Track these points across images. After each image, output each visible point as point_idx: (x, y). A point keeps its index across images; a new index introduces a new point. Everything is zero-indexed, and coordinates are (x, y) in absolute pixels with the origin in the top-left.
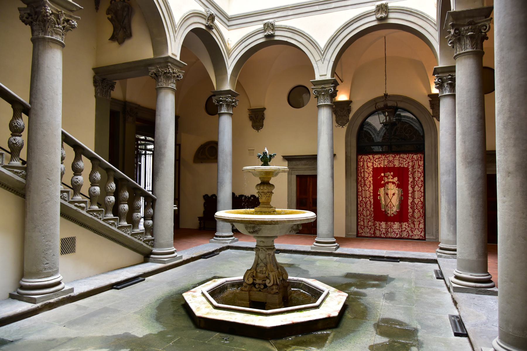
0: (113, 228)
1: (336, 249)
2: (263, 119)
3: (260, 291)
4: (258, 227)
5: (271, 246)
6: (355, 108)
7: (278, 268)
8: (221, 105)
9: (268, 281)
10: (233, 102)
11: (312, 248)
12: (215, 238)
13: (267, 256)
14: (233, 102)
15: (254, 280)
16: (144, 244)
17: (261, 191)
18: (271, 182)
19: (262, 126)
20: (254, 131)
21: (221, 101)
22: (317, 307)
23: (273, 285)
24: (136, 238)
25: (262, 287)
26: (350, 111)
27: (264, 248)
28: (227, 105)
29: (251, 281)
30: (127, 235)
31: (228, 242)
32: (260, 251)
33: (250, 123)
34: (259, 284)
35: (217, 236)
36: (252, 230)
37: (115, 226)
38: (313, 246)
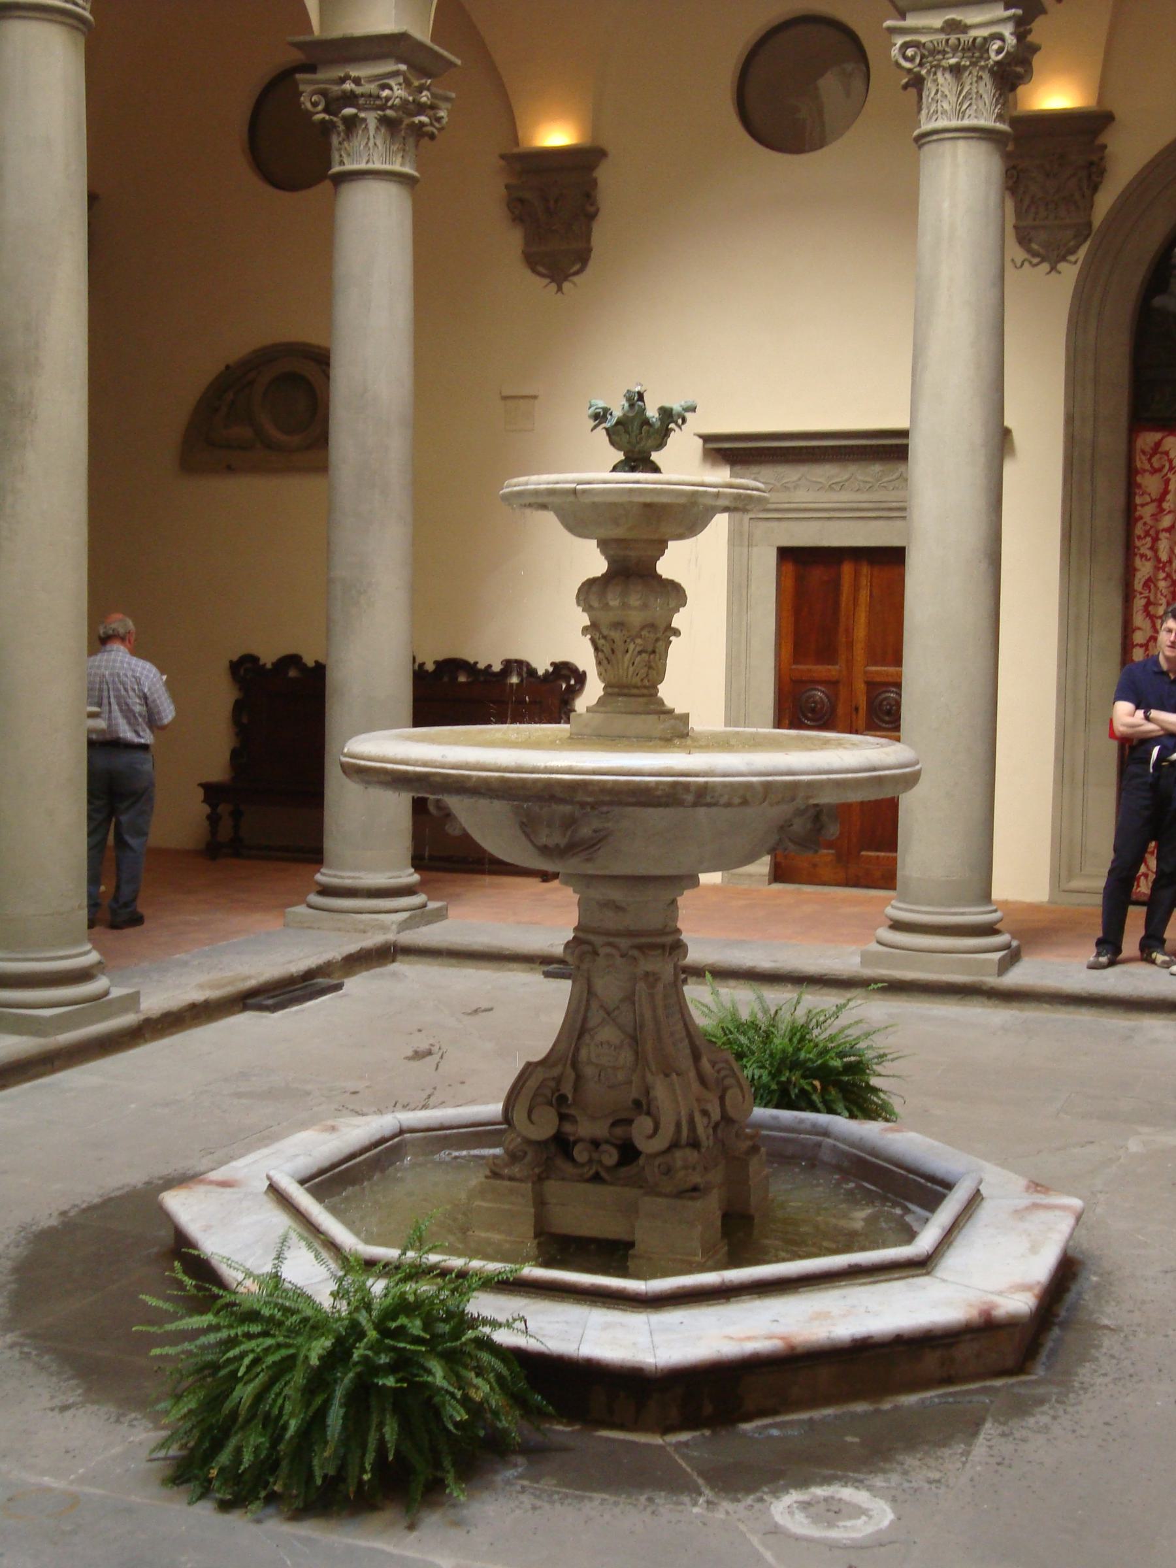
1: (1004, 966)
2: (592, 217)
3: (596, 1178)
4: (596, 824)
5: (662, 932)
6: (1128, 155)
7: (696, 1057)
8: (352, 124)
9: (643, 1124)
10: (421, 108)
11: (866, 958)
12: (313, 898)
13: (641, 986)
14: (421, 108)
15: (563, 1117)
17: (606, 618)
18: (665, 567)
19: (583, 257)
20: (538, 285)
21: (350, 99)
22: (922, 1265)
23: (674, 1145)
25: (610, 1157)
26: (1102, 172)
27: (624, 943)
28: (384, 121)
29: (544, 1127)
31: (386, 924)
32: (601, 961)
33: (513, 240)
34: (596, 1144)
35: (327, 891)
36: (557, 839)
38: (874, 947)
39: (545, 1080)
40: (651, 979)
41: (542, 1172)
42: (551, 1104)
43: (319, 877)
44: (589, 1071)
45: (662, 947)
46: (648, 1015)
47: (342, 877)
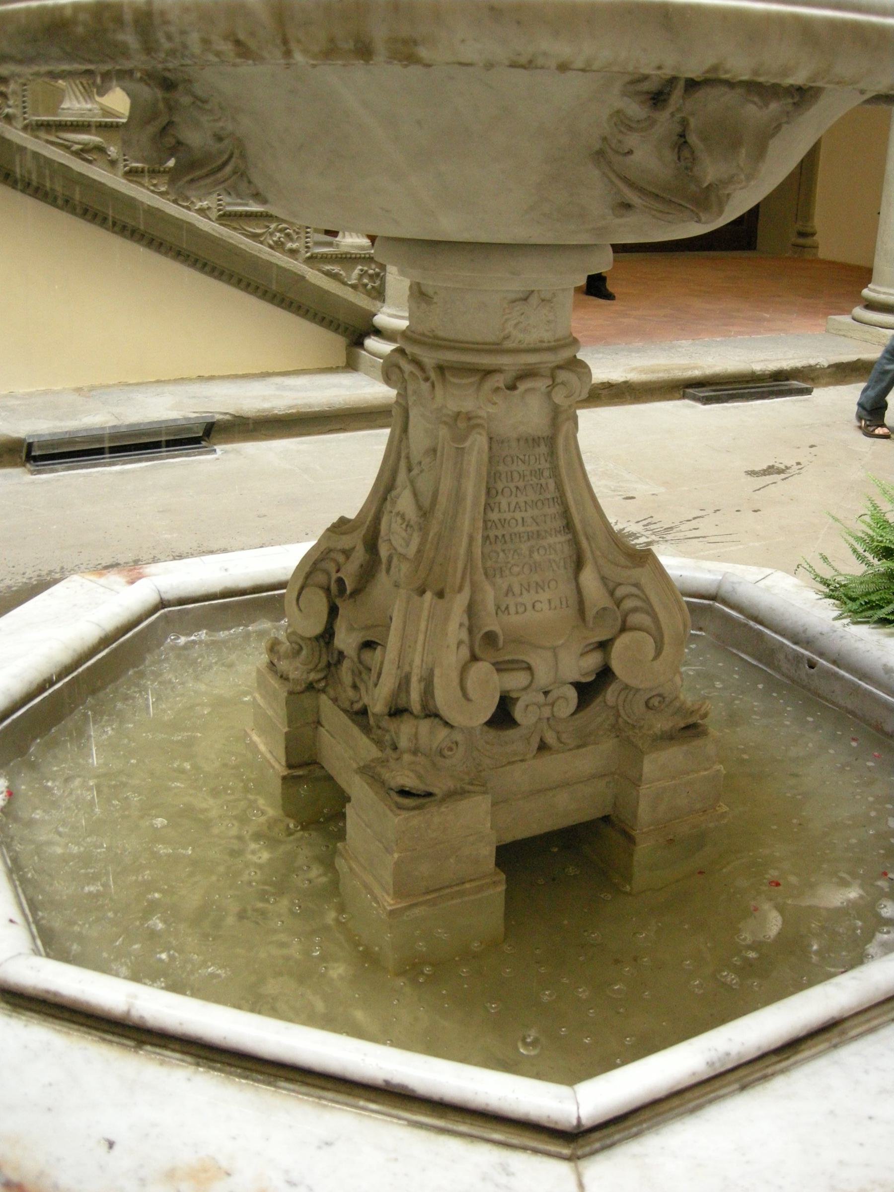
0: (97, 173)
7: (579, 564)
12: (859, 311)
16: (313, 276)
23: (397, 712)
24: (255, 237)
27: (429, 358)
30: (193, 217)
35: (871, 306)
37: (113, 163)
39: (330, 550)
40: (462, 425)
41: (319, 681)
42: (328, 590)
43: (865, 292)
44: (384, 551)
45: (487, 373)
46: (446, 485)
47: (879, 292)
